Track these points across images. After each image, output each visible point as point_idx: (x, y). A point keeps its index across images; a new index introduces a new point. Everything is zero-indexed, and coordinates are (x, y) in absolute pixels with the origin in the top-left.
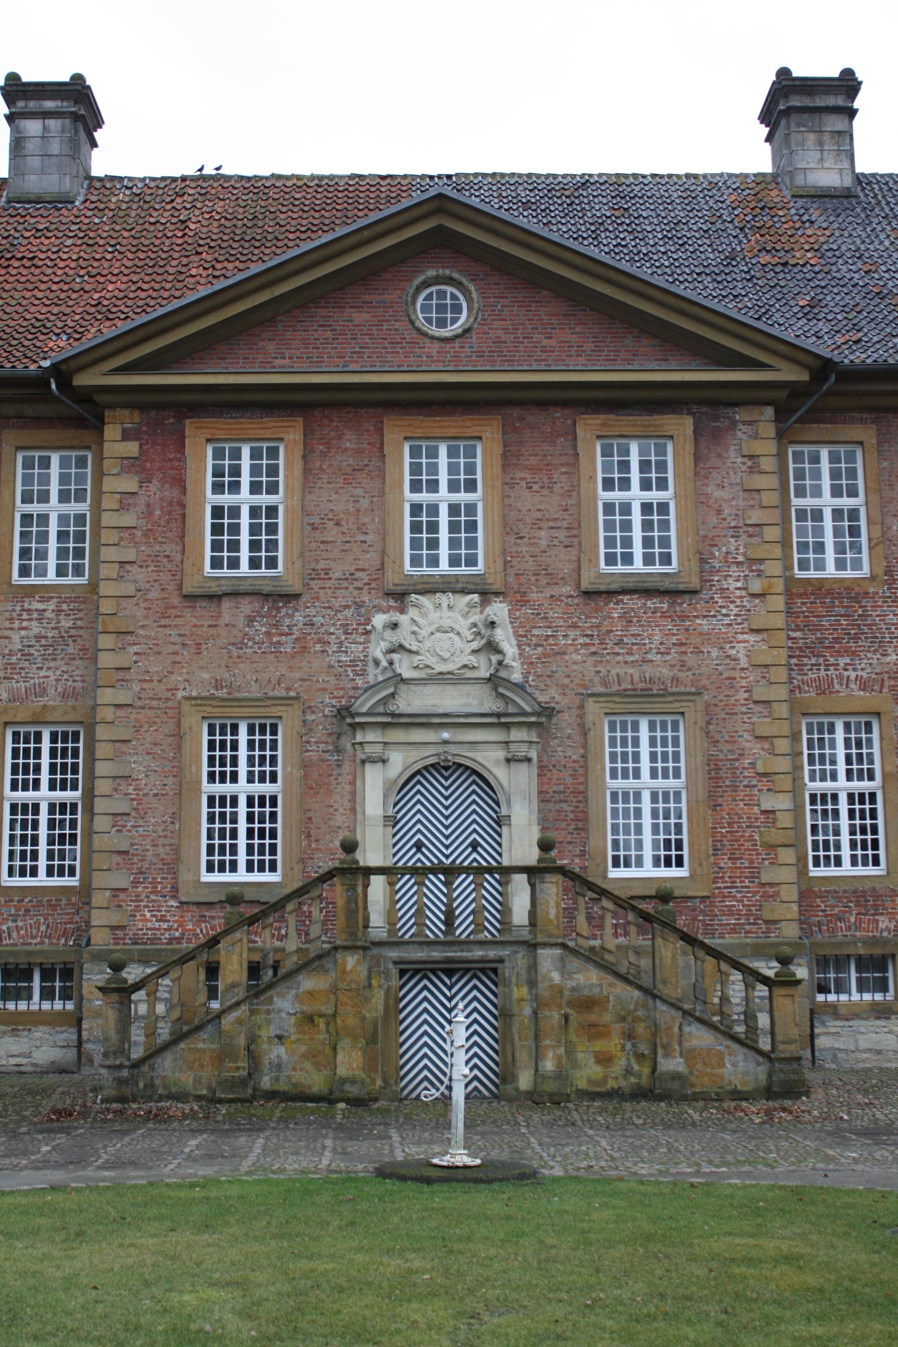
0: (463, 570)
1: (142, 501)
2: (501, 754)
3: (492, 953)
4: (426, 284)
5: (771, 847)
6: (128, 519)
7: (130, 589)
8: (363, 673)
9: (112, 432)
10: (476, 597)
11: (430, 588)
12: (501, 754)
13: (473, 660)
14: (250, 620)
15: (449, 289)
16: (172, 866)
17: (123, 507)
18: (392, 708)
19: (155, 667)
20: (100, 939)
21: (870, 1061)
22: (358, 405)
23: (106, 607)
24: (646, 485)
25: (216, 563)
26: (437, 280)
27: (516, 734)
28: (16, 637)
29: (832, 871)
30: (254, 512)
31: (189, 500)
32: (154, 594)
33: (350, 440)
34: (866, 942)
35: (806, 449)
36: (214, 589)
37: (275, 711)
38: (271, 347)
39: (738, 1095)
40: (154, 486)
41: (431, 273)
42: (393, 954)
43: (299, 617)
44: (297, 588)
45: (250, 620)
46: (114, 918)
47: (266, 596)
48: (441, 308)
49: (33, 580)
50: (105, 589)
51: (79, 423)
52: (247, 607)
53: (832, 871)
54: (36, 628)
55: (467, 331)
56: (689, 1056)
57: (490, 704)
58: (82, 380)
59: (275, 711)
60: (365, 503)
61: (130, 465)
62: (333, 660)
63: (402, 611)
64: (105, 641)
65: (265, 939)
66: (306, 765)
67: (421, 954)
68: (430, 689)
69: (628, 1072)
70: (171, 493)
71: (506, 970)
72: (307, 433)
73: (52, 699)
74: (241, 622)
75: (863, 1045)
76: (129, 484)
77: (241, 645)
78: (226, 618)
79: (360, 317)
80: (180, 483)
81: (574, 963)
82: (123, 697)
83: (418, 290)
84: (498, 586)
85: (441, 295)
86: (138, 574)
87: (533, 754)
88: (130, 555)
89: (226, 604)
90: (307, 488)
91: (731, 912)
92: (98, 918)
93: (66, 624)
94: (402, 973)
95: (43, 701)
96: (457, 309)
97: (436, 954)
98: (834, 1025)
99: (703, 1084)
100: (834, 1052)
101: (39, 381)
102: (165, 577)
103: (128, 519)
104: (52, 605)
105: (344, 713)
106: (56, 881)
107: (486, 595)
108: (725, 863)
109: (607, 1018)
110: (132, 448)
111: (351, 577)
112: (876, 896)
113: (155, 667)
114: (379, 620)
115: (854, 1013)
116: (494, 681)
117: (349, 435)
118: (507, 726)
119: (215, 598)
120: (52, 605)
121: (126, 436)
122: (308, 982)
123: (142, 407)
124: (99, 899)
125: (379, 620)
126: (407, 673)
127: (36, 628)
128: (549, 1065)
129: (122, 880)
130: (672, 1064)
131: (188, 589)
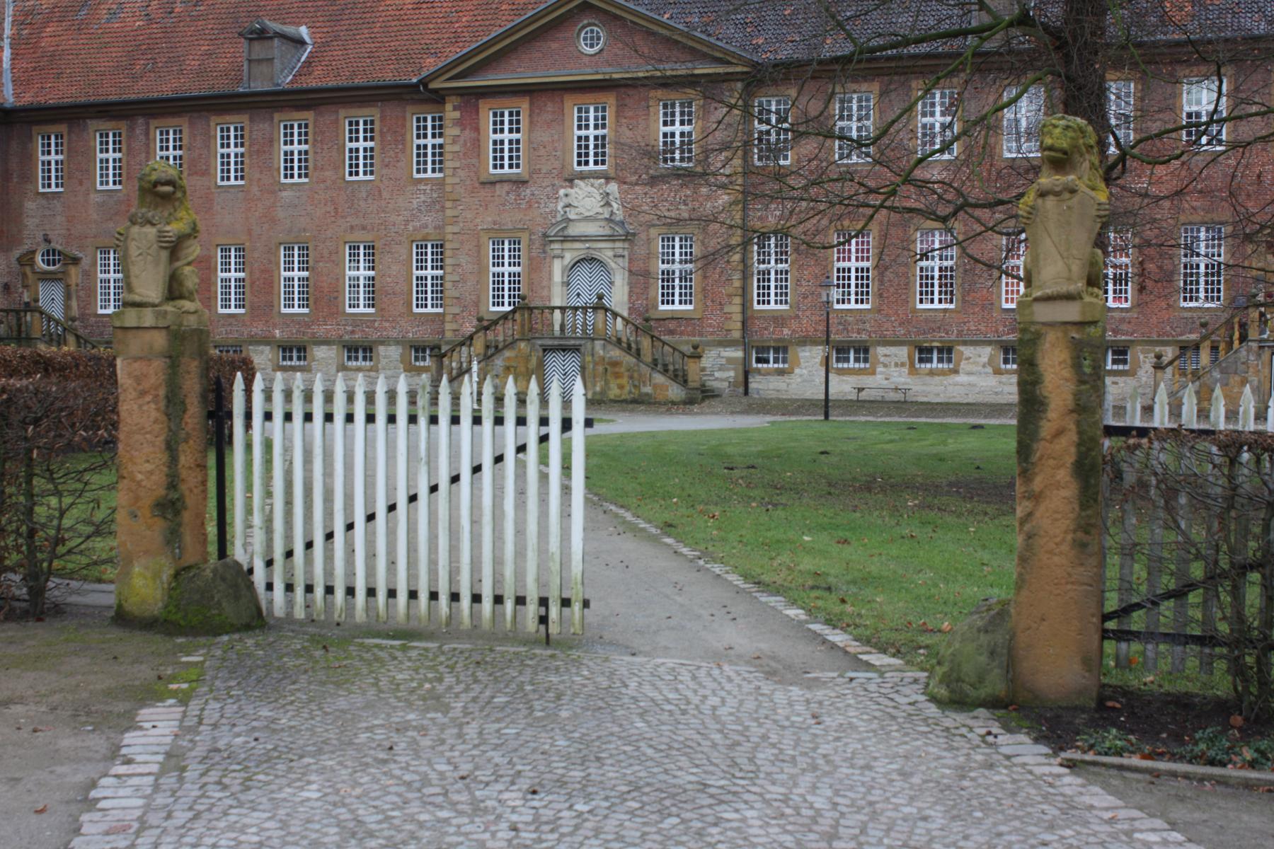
0: (600, 167)
1: (462, 139)
2: (610, 253)
3: (577, 342)
4: (584, 27)
5: (730, 296)
6: (456, 148)
7: (457, 180)
8: (555, 217)
9: (449, 107)
10: (603, 181)
11: (583, 177)
12: (610, 253)
13: (600, 210)
14: (508, 193)
15: (595, 29)
16: (477, 304)
17: (454, 142)
18: (566, 233)
19: (469, 215)
20: (449, 335)
21: (774, 395)
22: (554, 90)
23: (448, 189)
24: (682, 123)
25: (495, 167)
26: (589, 25)
27: (618, 245)
28: (415, 202)
29: (766, 307)
30: (511, 142)
31: (482, 138)
32: (468, 182)
33: (550, 106)
34: (775, 340)
35: (764, 99)
36: (492, 179)
37: (519, 234)
38: (515, 62)
39: (673, 403)
40: (467, 132)
41: (585, 22)
42: (540, 342)
43: (528, 191)
44: (526, 177)
45: (508, 193)
46: (454, 326)
47: (515, 182)
48: (592, 38)
49: (422, 175)
50: (449, 180)
51: (438, 102)
52: (506, 187)
53: (766, 307)
54: (423, 198)
55: (601, 51)
56: (655, 386)
57: (608, 232)
58: (433, 85)
59: (519, 234)
60: (556, 137)
61: (458, 123)
62: (542, 211)
63: (572, 187)
64: (449, 204)
65: (490, 333)
66: (530, 259)
67: (550, 342)
68: (582, 224)
69: (630, 392)
70: (474, 135)
71: (582, 349)
72: (531, 104)
73: (430, 230)
74: (504, 194)
75: (771, 387)
76: (456, 131)
77: (504, 205)
78: (498, 193)
79: (554, 45)
80: (477, 130)
81: (610, 347)
82: (456, 229)
83: (580, 31)
84: (613, 175)
85: (592, 31)
86: (461, 173)
87: (626, 253)
88: (457, 164)
89: (498, 186)
90: (531, 130)
91: (710, 325)
92: (448, 326)
93: (435, 195)
94: (544, 350)
95: (426, 231)
96: (599, 39)
97: (556, 343)
98: (758, 378)
99: (660, 398)
100: (758, 391)
101: (416, 86)
102: (472, 174)
103: (456, 148)
104: (429, 187)
105: (545, 235)
106: (435, 310)
107: (608, 179)
108: (709, 303)
109: (623, 370)
110: (457, 114)
111: (550, 172)
112: (783, 319)
113: (469, 215)
114: (562, 192)
115: (768, 373)
116: (609, 220)
117: (549, 104)
118: (614, 241)
119: (493, 183)
120: (429, 187)
121: (455, 109)
122: (507, 353)
123: (462, 95)
124: (448, 318)
125: (562, 192)
126: (572, 216)
127: (423, 198)
128: (598, 389)
129: (457, 310)
130: (647, 389)
131: (482, 179)
